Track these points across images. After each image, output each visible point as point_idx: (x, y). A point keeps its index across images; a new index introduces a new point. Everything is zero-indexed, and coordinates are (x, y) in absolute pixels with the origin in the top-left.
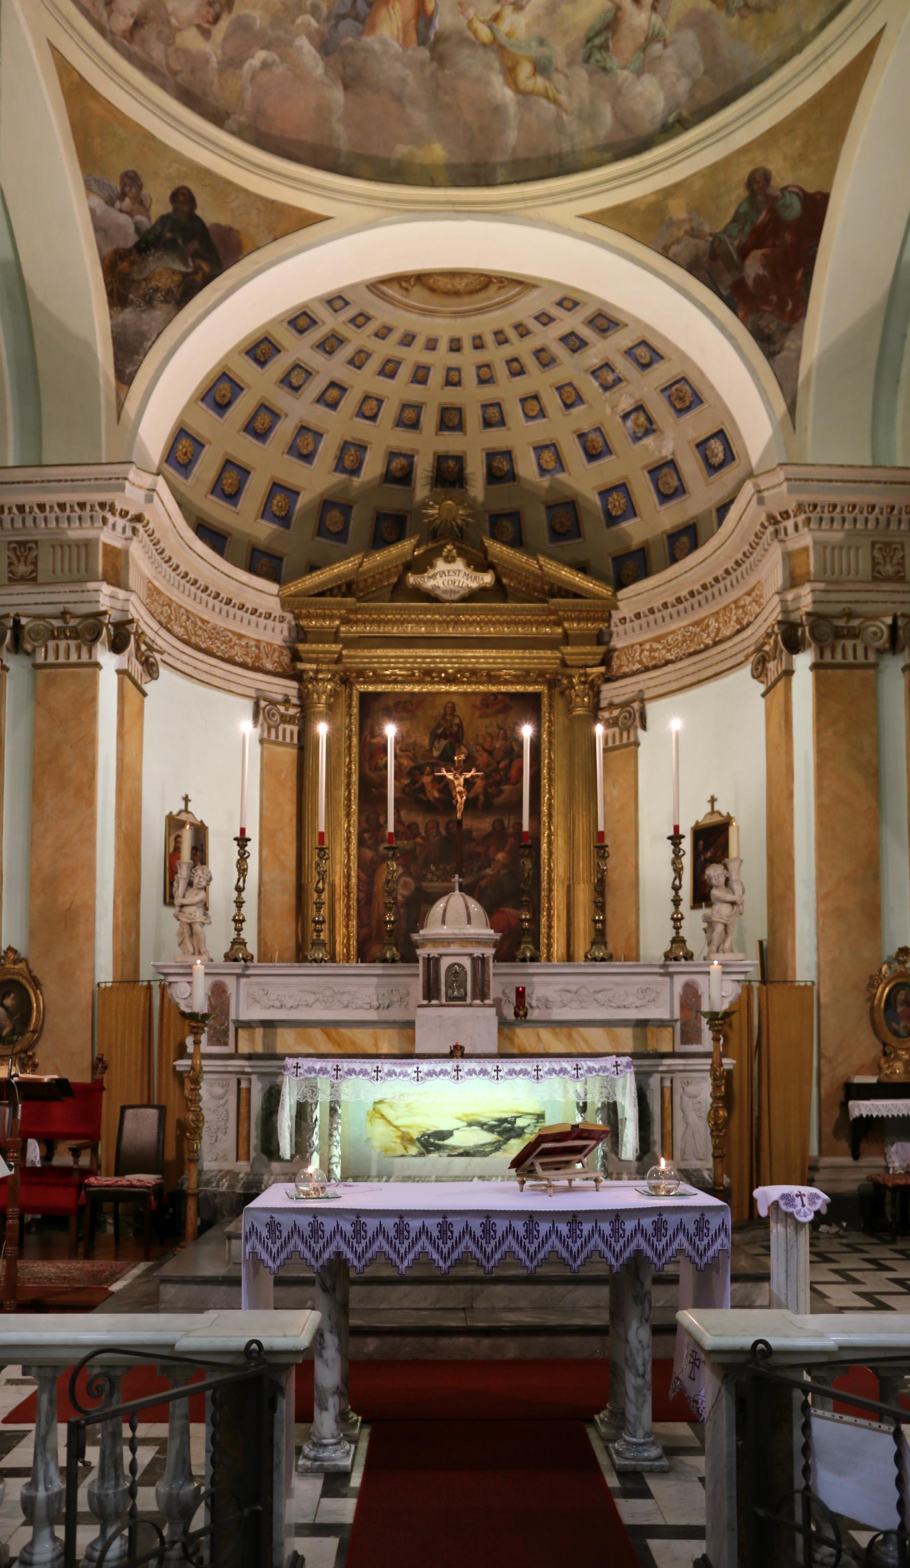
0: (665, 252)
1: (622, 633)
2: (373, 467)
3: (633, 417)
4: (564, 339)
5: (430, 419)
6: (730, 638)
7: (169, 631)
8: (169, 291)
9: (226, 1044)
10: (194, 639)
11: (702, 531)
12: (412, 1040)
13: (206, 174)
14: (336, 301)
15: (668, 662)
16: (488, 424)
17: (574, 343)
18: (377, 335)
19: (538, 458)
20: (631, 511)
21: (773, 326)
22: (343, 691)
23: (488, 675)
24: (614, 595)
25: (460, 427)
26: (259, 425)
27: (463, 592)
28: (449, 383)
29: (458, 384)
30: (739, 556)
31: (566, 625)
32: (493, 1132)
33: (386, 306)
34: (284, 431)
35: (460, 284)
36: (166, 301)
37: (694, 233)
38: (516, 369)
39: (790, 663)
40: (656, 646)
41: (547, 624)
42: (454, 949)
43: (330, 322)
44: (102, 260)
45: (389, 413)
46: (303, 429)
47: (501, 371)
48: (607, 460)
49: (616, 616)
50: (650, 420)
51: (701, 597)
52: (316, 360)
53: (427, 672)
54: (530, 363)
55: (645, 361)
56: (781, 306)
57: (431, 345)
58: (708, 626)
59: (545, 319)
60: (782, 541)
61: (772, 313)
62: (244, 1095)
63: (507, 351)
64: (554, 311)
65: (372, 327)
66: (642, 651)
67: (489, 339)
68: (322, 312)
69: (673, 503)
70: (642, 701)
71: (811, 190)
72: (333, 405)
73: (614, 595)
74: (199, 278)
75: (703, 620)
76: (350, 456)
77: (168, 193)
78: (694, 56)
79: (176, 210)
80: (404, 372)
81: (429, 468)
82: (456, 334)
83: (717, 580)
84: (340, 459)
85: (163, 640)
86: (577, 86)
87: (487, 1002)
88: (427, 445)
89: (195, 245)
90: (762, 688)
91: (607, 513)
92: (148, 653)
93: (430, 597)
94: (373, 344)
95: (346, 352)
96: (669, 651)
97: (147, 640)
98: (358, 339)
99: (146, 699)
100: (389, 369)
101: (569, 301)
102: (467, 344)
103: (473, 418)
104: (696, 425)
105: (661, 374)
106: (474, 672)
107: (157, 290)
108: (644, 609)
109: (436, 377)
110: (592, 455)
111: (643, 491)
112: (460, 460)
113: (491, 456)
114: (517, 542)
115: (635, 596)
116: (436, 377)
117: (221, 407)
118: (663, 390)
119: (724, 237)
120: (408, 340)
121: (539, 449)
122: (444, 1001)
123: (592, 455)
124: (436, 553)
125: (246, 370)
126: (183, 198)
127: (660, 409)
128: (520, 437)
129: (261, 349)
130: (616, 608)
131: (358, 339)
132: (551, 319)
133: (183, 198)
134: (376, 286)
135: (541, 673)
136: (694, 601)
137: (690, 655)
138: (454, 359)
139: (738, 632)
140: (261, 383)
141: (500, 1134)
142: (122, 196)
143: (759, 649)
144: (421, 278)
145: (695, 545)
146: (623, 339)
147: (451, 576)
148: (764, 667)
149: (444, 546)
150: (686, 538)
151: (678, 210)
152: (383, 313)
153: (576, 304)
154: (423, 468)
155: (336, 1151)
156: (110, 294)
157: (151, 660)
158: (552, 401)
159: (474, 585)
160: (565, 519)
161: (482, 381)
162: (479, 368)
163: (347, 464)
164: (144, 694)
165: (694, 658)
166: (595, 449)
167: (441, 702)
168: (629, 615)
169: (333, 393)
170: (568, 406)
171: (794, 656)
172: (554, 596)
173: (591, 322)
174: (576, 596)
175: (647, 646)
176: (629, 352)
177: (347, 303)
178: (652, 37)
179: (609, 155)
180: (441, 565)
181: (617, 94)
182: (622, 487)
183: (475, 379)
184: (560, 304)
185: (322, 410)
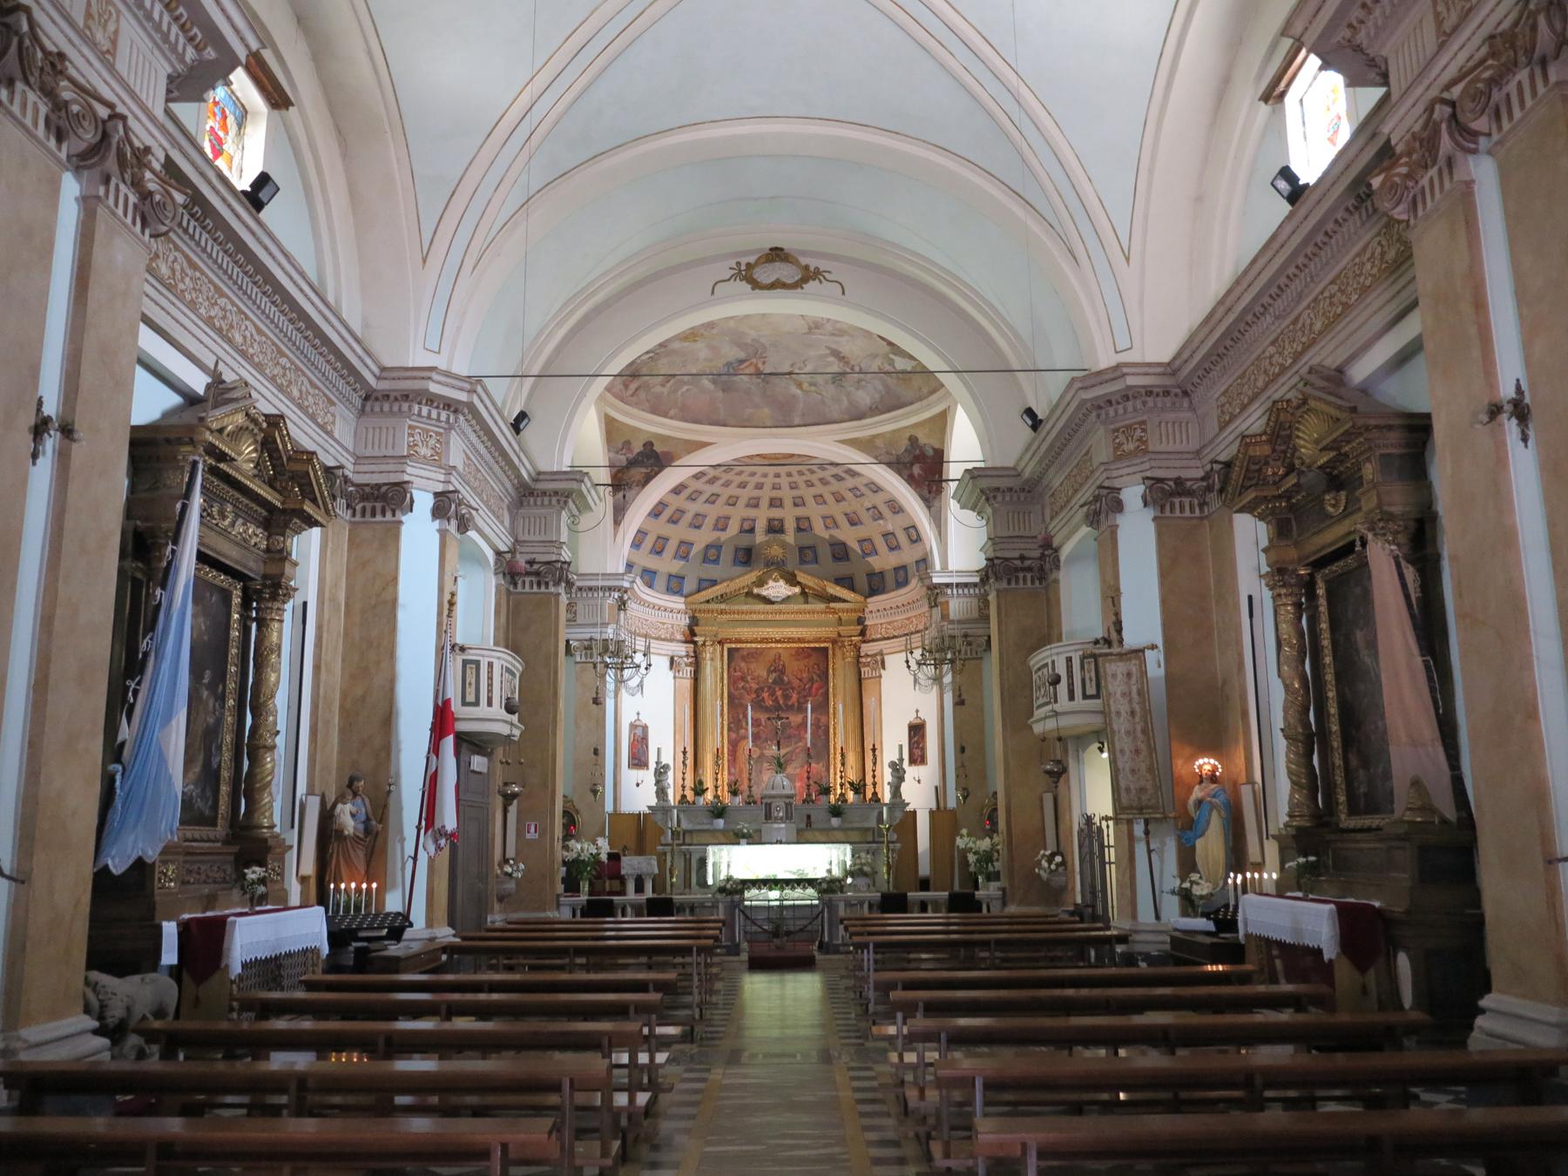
2: (733, 528)
5: (764, 503)
16: (796, 505)
22: (718, 648)
25: (781, 505)
38: (810, 484)
43: (712, 473)
57: (765, 475)
76: (721, 524)
78: (880, 387)
86: (830, 391)
88: (762, 516)
93: (767, 601)
100: (743, 485)
103: (788, 502)
109: (767, 487)
112: (781, 521)
113: (798, 519)
115: (875, 602)
116: (767, 487)
121: (824, 518)
126: (649, 445)
128: (813, 511)
129: (677, 490)
133: (649, 445)
147: (777, 589)
154: (761, 526)
160: (840, 552)
166: (853, 522)
167: (772, 653)
174: (845, 601)
178: (860, 381)
180: (771, 583)
181: (849, 395)
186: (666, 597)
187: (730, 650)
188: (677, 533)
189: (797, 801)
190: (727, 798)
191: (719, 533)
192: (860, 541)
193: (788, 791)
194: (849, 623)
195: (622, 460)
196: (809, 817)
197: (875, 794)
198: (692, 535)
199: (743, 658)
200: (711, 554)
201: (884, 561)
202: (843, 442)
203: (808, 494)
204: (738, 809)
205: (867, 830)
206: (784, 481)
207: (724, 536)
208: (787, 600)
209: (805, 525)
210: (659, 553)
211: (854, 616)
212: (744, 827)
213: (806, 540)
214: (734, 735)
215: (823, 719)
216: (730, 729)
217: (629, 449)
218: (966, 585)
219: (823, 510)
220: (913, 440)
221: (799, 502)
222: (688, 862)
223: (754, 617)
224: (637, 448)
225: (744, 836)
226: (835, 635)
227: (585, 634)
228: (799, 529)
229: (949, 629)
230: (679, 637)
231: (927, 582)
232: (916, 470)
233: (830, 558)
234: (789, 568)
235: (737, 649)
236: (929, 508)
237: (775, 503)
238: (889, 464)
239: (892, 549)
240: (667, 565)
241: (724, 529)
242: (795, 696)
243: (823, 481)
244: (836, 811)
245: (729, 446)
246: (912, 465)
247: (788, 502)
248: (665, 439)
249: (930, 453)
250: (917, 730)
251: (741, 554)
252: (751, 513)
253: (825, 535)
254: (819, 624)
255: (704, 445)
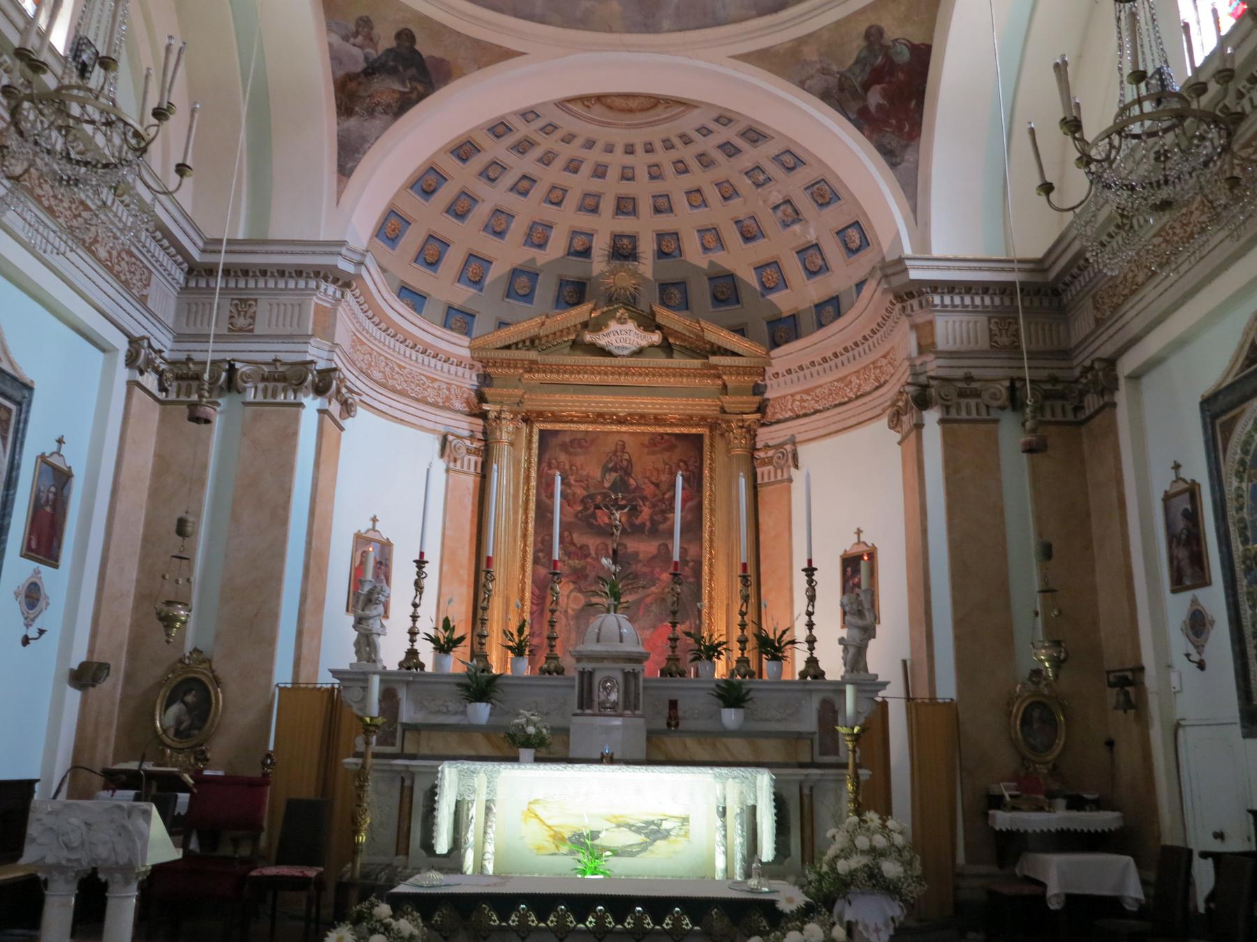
0: (801, 84)
1: (775, 386)
2: (557, 247)
3: (782, 208)
4: (721, 147)
5: (607, 206)
6: (869, 393)
7: (368, 376)
8: (389, 105)
9: (393, 745)
10: (391, 382)
11: (844, 303)
12: (566, 745)
13: (425, 20)
14: (529, 115)
15: (816, 412)
16: (657, 210)
17: (730, 150)
18: (563, 140)
19: (702, 239)
20: (784, 283)
21: (894, 144)
23: (655, 418)
24: (768, 353)
25: (634, 212)
26: (459, 209)
27: (633, 348)
28: (624, 177)
29: (632, 179)
30: (874, 326)
31: (725, 377)
32: (640, 833)
33: (571, 118)
34: (481, 213)
35: (633, 104)
36: (386, 113)
37: (825, 71)
38: (682, 168)
39: (921, 418)
40: (805, 397)
41: (709, 377)
42: (606, 664)
43: (523, 130)
44: (335, 83)
45: (572, 200)
46: (497, 211)
47: (669, 170)
48: (760, 243)
49: (770, 371)
50: (796, 212)
51: (844, 358)
52: (510, 159)
53: (601, 415)
54: (694, 165)
55: (790, 166)
56: (900, 128)
57: (609, 149)
58: (851, 382)
59: (704, 131)
60: (909, 316)
61: (893, 133)
62: (407, 792)
63: (674, 155)
64: (712, 126)
65: (559, 134)
66: (794, 401)
67: (658, 145)
68: (517, 123)
69: (819, 278)
70: (794, 443)
71: (916, 41)
72: (525, 193)
73: (768, 353)
74: (414, 96)
75: (846, 377)
76: (538, 236)
77: (394, 33)
79: (399, 45)
80: (586, 169)
81: (605, 247)
82: (631, 141)
83: (856, 344)
84: (529, 235)
85: (359, 384)
87: (637, 712)
88: (604, 227)
89: (412, 71)
90: (898, 437)
91: (762, 284)
92: (348, 395)
93: (604, 352)
94: (559, 147)
95: (537, 152)
96: (817, 402)
97: (348, 384)
98: (546, 143)
99: (343, 434)
100: (573, 166)
101: (724, 119)
102: (639, 149)
103: (645, 206)
104: (835, 217)
105: (803, 176)
106: (642, 416)
107: (378, 104)
108: (794, 367)
109: (613, 174)
110: (748, 238)
111: (793, 268)
112: (633, 238)
113: (660, 236)
114: (685, 305)
116: (613, 174)
117: (428, 193)
118: (806, 189)
119: (849, 74)
120: (590, 144)
121: (702, 231)
122: (596, 711)
123: (748, 238)
124: (609, 315)
125: (450, 165)
126: (405, 36)
127: (804, 203)
128: (685, 221)
129: (464, 150)
130: (770, 365)
131: (546, 143)
132: (710, 132)
133: (405, 36)
134: (563, 104)
135: (703, 418)
136: (838, 361)
137: (836, 406)
138: (628, 161)
139: (877, 388)
140: (462, 176)
141: (647, 835)
142: (356, 34)
143: (894, 404)
144: (600, 98)
145: (838, 314)
146: (771, 149)
147: (623, 335)
148: (898, 419)
149: (617, 310)
150: (830, 309)
151: (810, 53)
152: (567, 123)
153: (730, 121)
154: (601, 246)
155: (490, 848)
156: (339, 107)
157: (350, 401)
158: (712, 195)
159: (644, 343)
160: (725, 289)
161: (652, 177)
162: (649, 167)
163: (535, 240)
164: (342, 429)
165: (838, 408)
168: (781, 370)
169: (525, 184)
170: (725, 198)
171: (924, 413)
172: (714, 354)
173: (743, 135)
175: (798, 397)
176: (776, 158)
177: (538, 116)
179: (754, 13)
180: (614, 326)
182: (775, 264)
183: (647, 176)
184: (717, 120)
185: (514, 197)
186: (439, 331)
187: (543, 433)
188: (466, 237)
189: (651, 670)
190: (498, 660)
191: (534, 252)
192: (759, 269)
193: (630, 647)
194: (739, 391)
195: (357, 58)
196: (673, 704)
197: (812, 662)
198: (488, 246)
199: (564, 447)
200: (521, 284)
201: (799, 294)
202: (747, 58)
203: (676, 186)
204: (519, 683)
205: (799, 736)
206: (640, 161)
207: (542, 257)
208: (640, 352)
209: (670, 246)
210: (433, 265)
211: (748, 381)
212: (530, 721)
213: (671, 271)
214: (543, 571)
215: (692, 550)
216: (536, 561)
217: (370, 39)
218: (968, 288)
219: (702, 217)
220: (874, 36)
221: (662, 206)
222: (406, 794)
223: (586, 378)
224: (386, 41)
225: (527, 742)
226: (713, 412)
227: (263, 352)
228: (661, 254)
229: (933, 366)
230: (458, 405)
231: (897, 281)
232: (875, 98)
233: (708, 299)
234: (643, 306)
235: (556, 433)
236: (893, 165)
237: (625, 206)
238: (825, 96)
239: (812, 273)
240: (444, 286)
241: (541, 246)
242: (646, 512)
243: (705, 161)
244: (731, 694)
245: (548, 70)
246: (866, 87)
247: (645, 206)
248: (439, 31)
249: (904, 56)
250: (856, 566)
251: (568, 289)
252: (585, 222)
253: (704, 264)
254: (691, 393)
255: (507, 54)
